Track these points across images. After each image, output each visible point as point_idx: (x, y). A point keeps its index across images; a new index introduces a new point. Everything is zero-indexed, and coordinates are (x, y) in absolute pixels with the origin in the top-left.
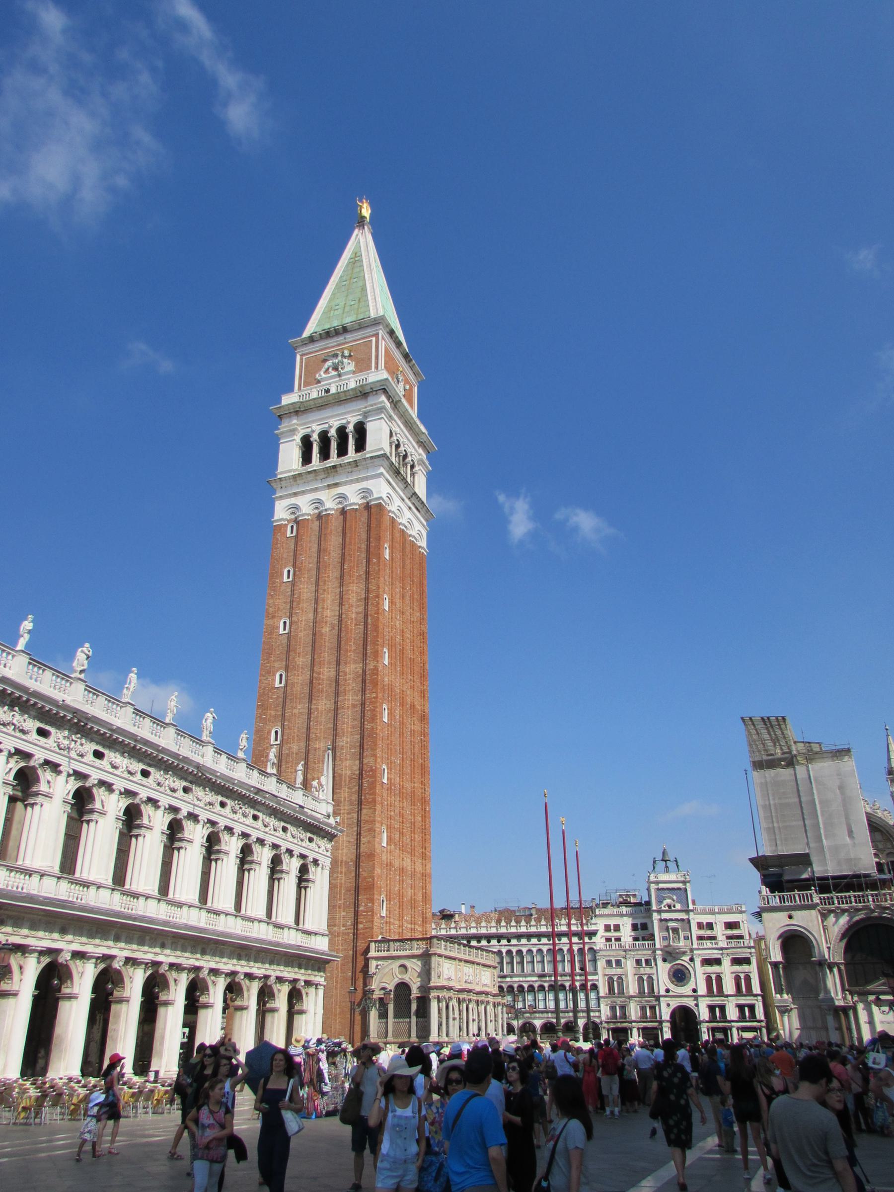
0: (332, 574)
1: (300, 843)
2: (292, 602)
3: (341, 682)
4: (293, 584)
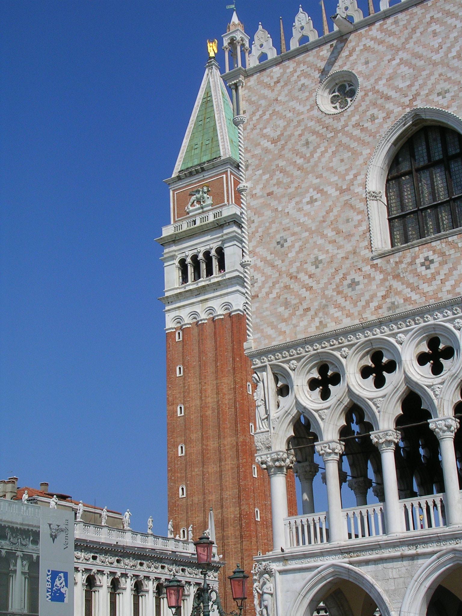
0: (211, 369)
1: (195, 577)
4: (184, 378)
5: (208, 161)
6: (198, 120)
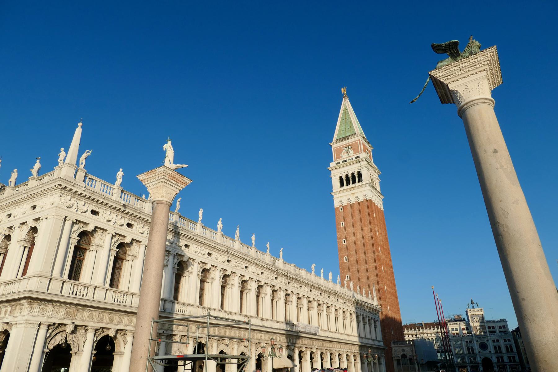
0: (358, 223)
2: (346, 233)
6: (342, 119)
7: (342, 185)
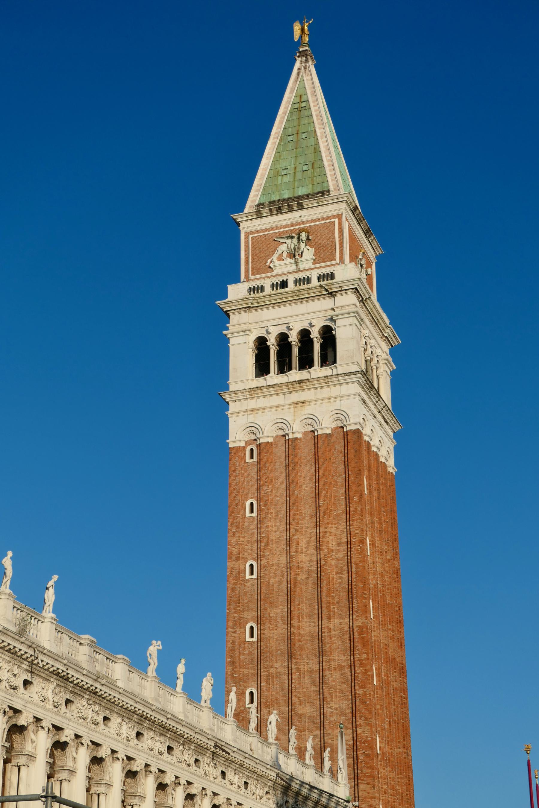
0: (307, 510)
2: (259, 542)
3: (326, 640)
4: (259, 520)
5: (307, 196)
7: (262, 367)
